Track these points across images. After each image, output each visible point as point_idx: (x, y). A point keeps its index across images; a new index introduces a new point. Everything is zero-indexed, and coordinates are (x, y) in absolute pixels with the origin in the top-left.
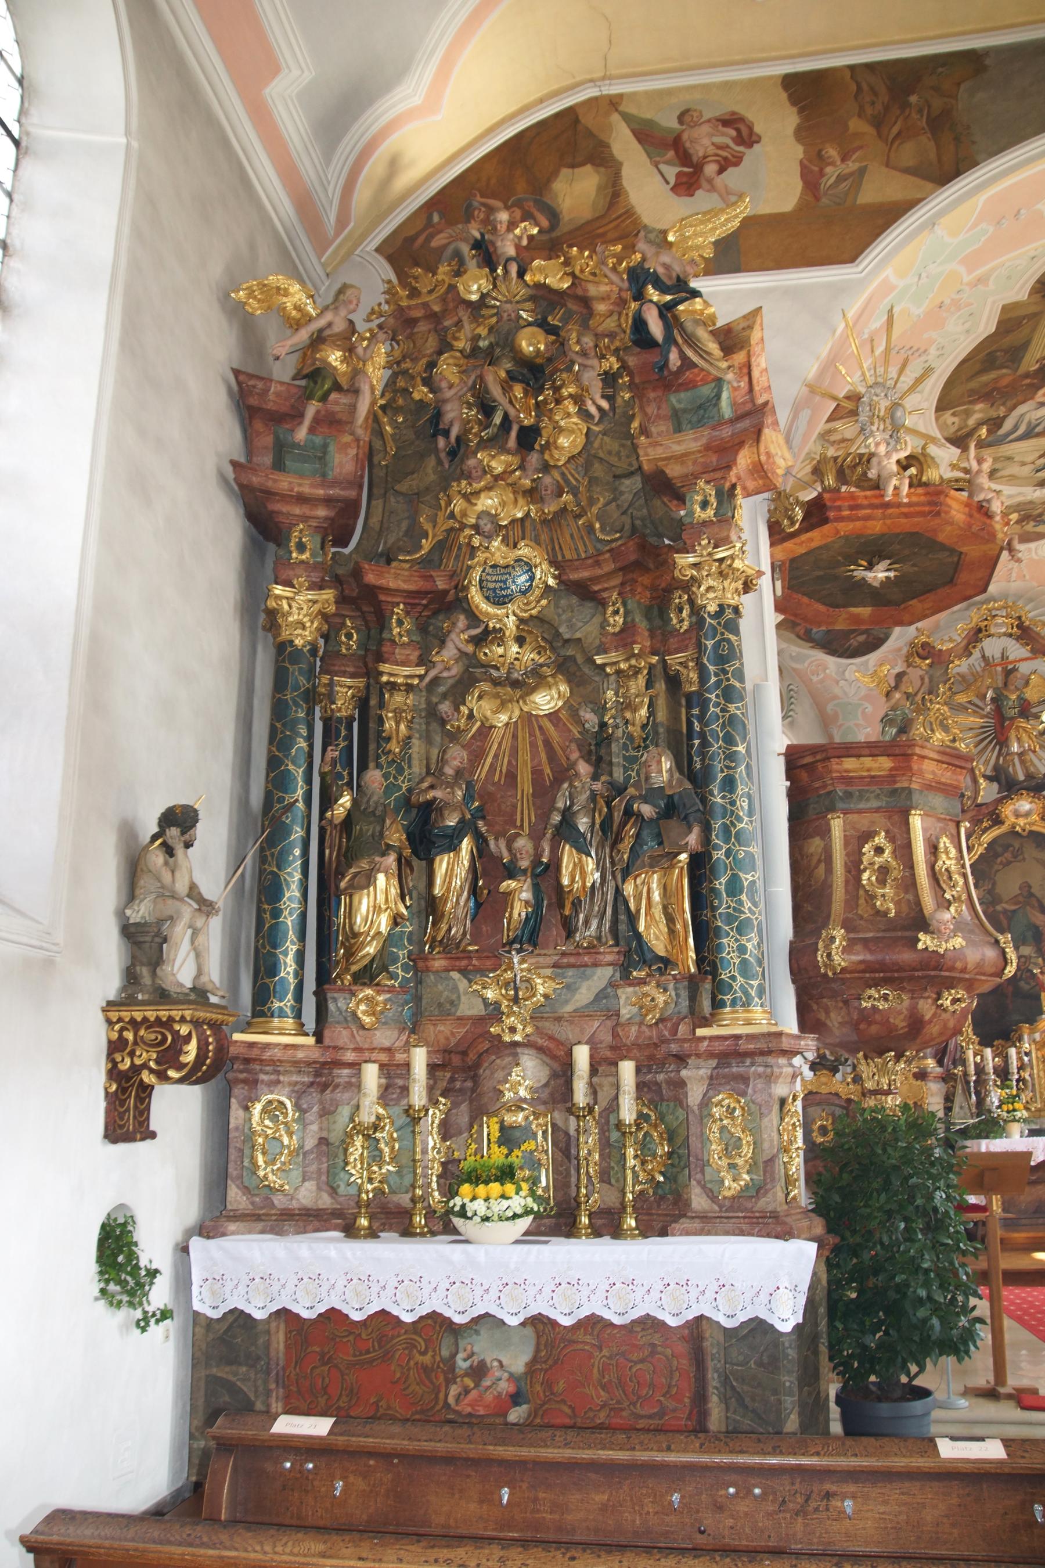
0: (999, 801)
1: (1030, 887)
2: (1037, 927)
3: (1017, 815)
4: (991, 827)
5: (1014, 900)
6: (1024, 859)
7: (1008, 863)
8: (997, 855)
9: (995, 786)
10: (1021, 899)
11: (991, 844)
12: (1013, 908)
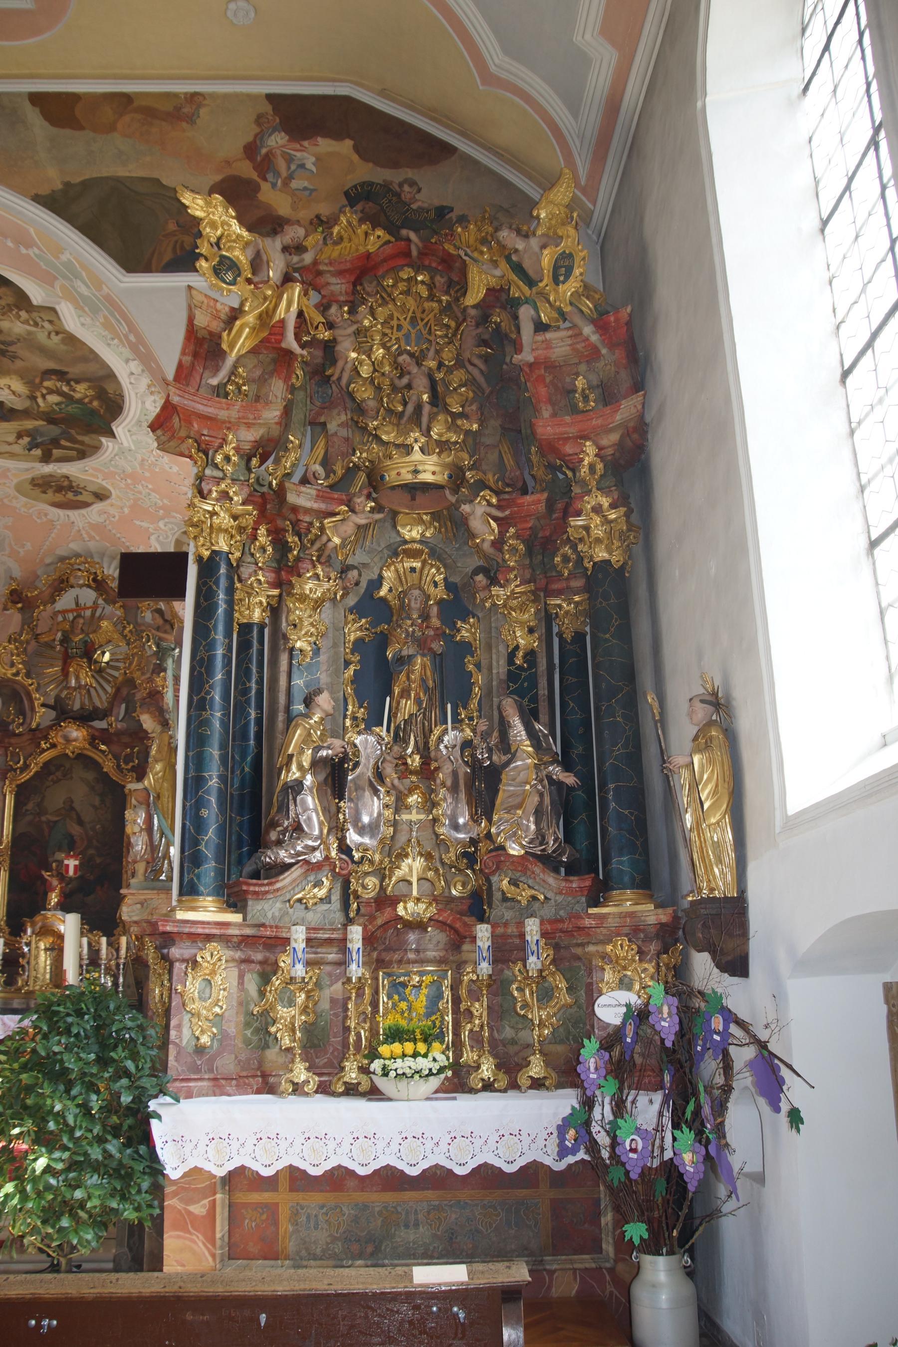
0: (50, 727)
1: (72, 802)
2: (72, 837)
3: (68, 740)
4: (48, 749)
6: (72, 778)
8: (50, 773)
9: (53, 714)
11: (46, 764)
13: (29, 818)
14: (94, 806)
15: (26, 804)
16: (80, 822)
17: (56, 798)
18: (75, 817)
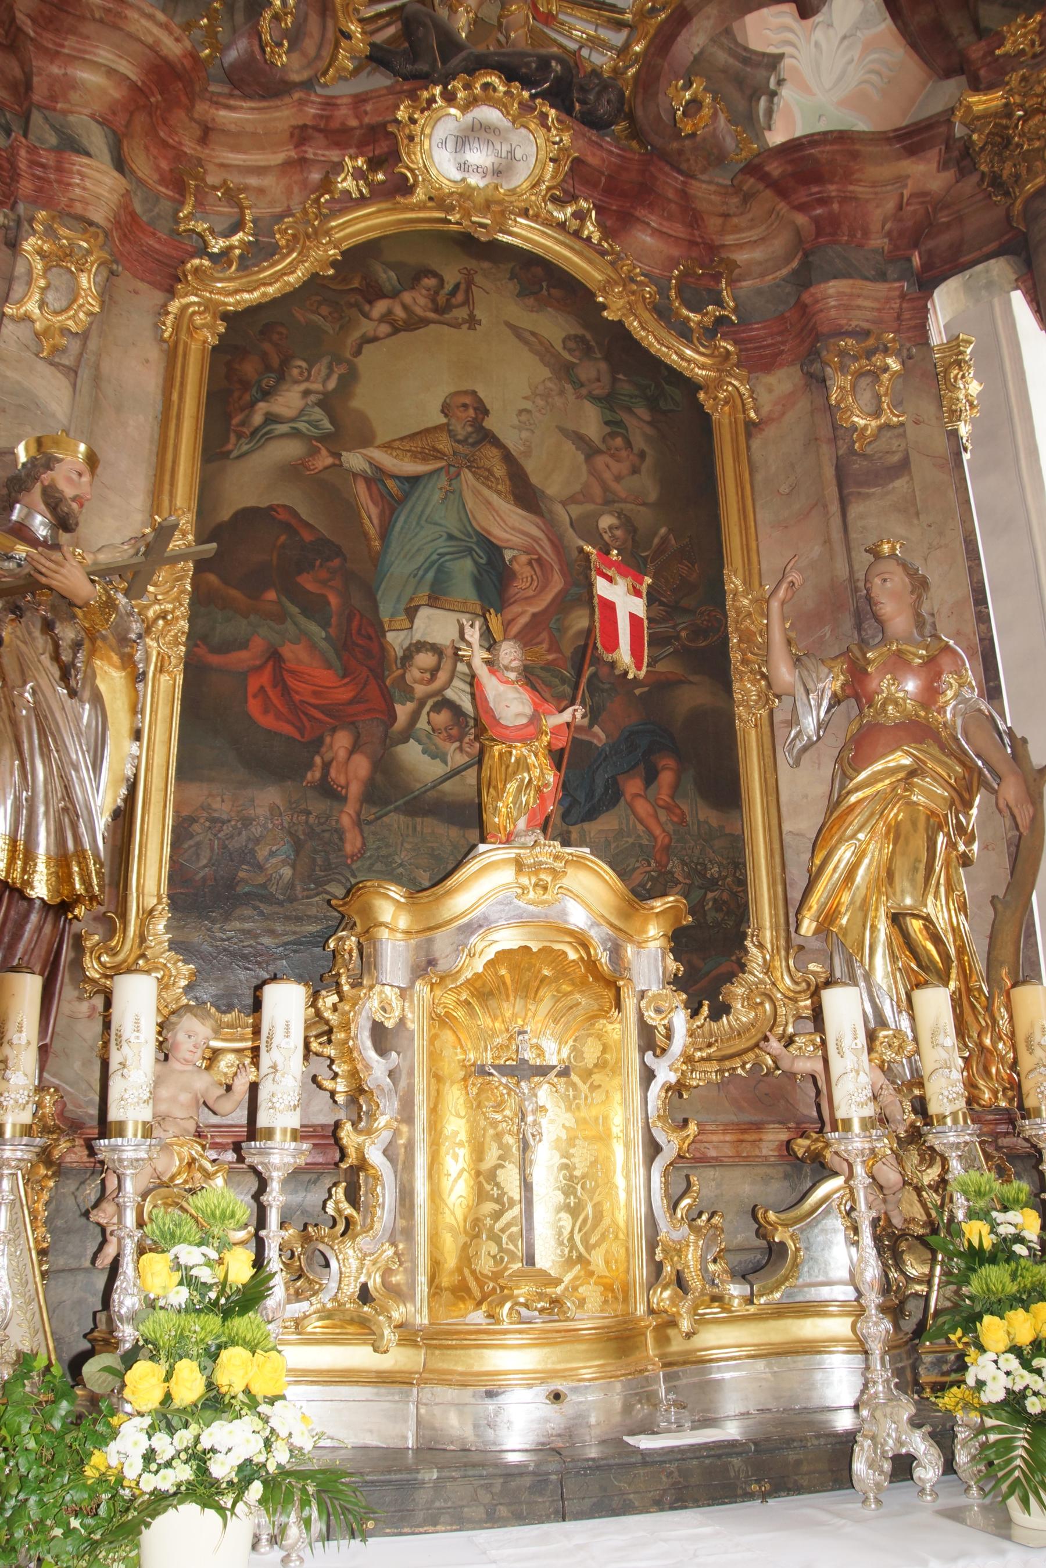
1: (483, 411)
2: (493, 550)
5: (419, 442)
6: (472, 322)
7: (413, 323)
8: (373, 292)
10: (444, 444)
11: (359, 257)
12: (411, 467)
13: (290, 450)
14: (580, 439)
15: (266, 394)
16: (525, 495)
17: (406, 388)
18: (500, 470)
